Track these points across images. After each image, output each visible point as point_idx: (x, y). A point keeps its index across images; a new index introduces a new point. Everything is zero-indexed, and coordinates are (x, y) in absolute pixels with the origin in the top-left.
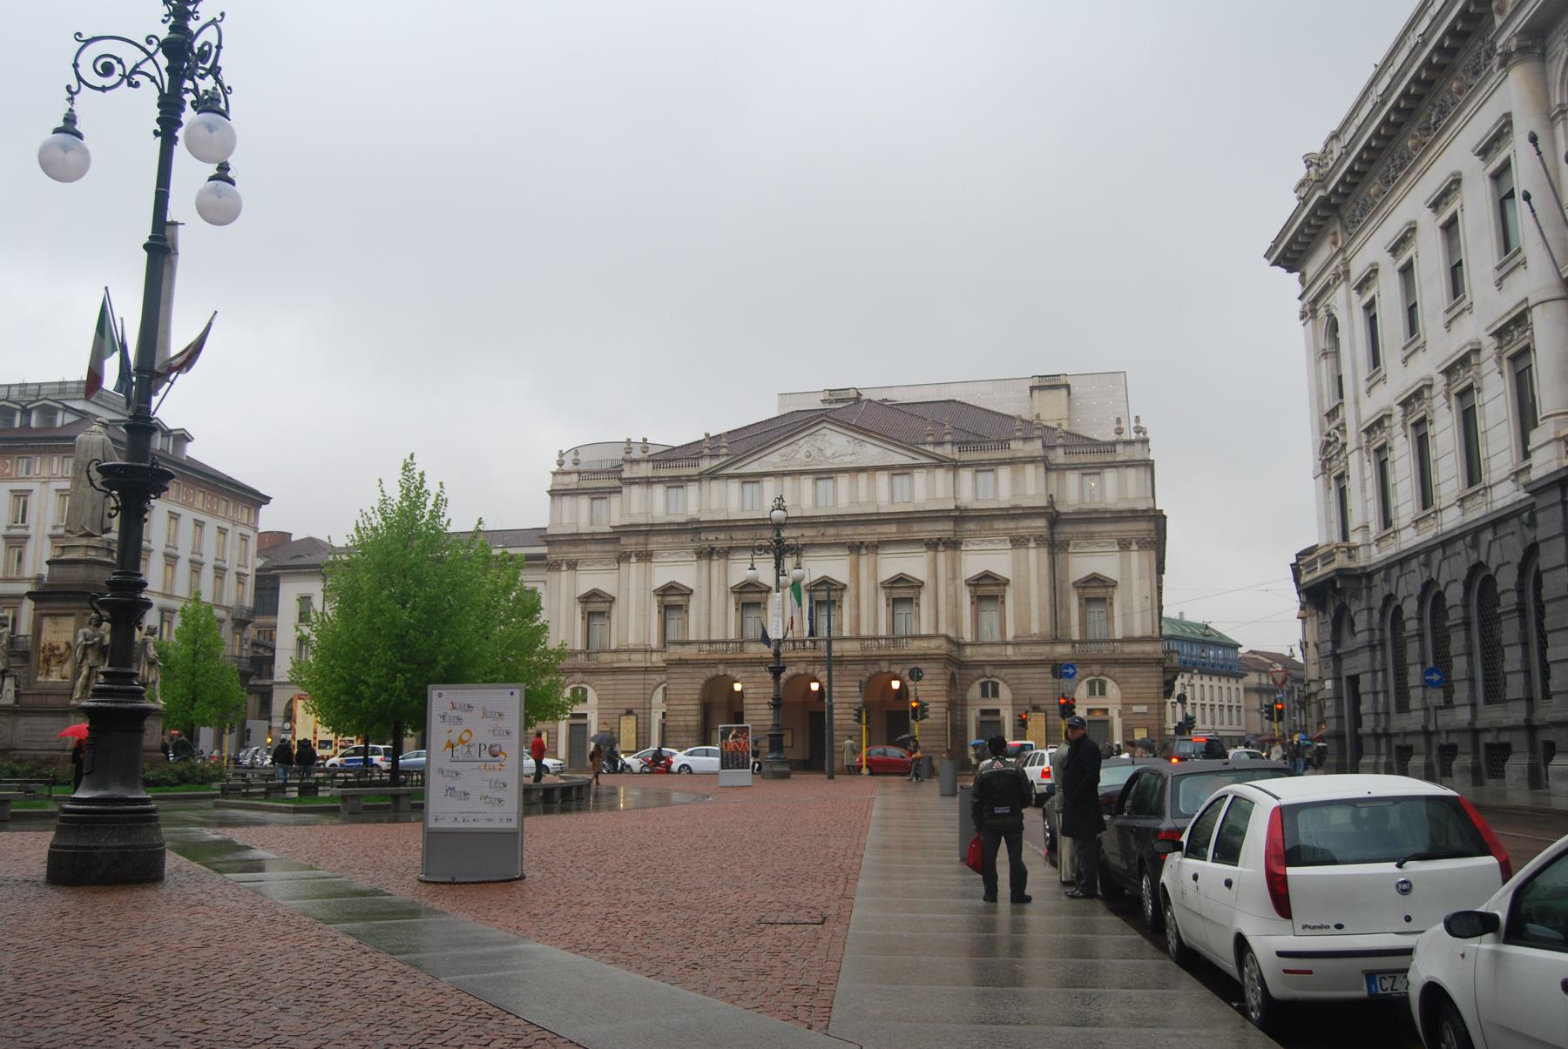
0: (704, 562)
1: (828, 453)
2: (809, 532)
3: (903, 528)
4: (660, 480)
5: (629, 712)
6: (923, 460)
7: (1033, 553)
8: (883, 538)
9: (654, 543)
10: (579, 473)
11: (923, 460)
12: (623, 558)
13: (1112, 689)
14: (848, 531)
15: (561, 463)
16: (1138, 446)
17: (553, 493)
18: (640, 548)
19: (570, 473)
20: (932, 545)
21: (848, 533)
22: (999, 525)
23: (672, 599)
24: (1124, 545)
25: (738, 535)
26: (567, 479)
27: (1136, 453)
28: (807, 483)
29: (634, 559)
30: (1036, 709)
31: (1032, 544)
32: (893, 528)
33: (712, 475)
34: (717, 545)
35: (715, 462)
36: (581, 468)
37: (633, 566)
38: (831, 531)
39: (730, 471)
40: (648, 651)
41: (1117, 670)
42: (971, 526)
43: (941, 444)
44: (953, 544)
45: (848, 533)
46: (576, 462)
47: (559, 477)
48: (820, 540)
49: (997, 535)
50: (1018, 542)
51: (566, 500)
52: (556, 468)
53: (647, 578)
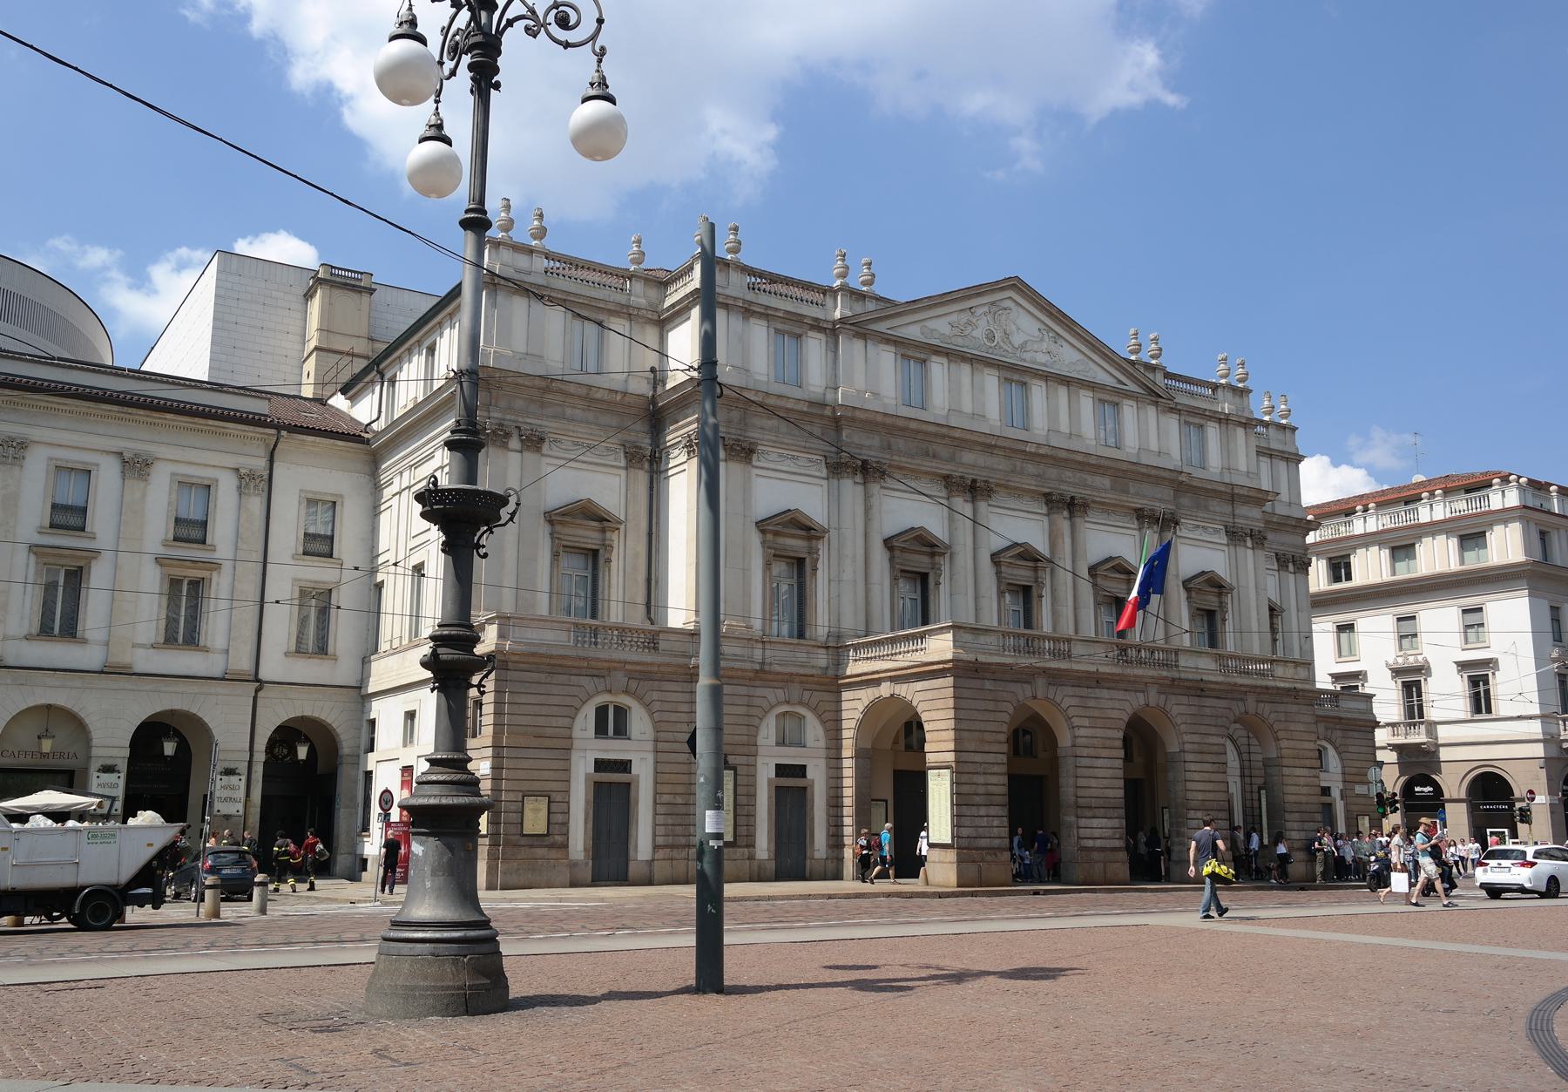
1: (1017, 339)
2: (1000, 463)
4: (767, 315)
6: (1132, 387)
7: (1250, 552)
9: (761, 429)
11: (1132, 387)
14: (1053, 472)
19: (530, 251)
20: (1143, 517)
22: (1216, 505)
23: (792, 544)
25: (901, 444)
26: (522, 261)
27: (1275, 441)
28: (991, 380)
32: (1107, 482)
35: (859, 308)
38: (1031, 468)
39: (882, 327)
42: (1185, 501)
44: (1168, 522)
49: (1213, 521)
50: (1235, 535)
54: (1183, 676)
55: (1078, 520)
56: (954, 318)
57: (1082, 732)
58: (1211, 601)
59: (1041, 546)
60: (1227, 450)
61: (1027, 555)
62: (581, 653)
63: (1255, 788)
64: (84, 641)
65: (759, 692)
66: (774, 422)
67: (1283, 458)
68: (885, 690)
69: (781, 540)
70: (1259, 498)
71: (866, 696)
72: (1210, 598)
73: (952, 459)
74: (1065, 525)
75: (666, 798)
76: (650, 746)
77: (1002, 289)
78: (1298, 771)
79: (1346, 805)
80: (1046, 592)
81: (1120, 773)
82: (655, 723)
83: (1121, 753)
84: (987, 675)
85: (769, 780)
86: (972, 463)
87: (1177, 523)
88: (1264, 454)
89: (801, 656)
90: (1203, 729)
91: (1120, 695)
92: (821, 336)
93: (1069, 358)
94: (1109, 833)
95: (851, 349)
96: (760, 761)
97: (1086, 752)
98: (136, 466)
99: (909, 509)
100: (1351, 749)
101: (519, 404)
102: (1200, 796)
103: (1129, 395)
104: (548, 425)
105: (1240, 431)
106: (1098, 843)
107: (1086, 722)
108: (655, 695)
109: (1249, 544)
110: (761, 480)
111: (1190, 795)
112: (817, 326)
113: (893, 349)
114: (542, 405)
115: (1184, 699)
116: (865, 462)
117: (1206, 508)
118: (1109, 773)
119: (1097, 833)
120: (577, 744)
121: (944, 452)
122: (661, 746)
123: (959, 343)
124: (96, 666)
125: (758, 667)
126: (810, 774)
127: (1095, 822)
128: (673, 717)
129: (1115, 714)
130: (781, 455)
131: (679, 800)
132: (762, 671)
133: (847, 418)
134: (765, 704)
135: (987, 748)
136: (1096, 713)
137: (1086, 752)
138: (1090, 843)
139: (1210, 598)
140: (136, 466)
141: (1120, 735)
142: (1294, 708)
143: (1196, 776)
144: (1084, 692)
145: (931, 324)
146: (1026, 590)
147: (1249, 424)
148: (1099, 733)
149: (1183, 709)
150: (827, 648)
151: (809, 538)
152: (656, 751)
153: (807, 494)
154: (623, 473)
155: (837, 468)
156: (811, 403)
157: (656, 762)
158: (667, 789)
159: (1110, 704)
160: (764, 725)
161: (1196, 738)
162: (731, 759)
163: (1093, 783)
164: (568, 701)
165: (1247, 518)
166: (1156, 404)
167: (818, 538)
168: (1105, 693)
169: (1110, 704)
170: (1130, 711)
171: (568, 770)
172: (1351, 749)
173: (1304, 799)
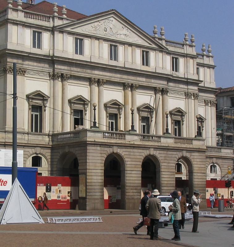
0: (57, 81)
3: (148, 80)
4: (29, 26)
8: (141, 84)
9: (28, 64)
11: (154, 46)
14: (125, 77)
21: (126, 79)
24: (206, 103)
32: (144, 79)
33: (62, 30)
34: (64, 72)
38: (119, 76)
39: (69, 29)
41: (220, 161)
43: (161, 39)
44: (164, 92)
45: (126, 79)
48: (113, 79)
50: (187, 95)
54: (162, 145)
55: (134, 92)
58: (178, 118)
59: (121, 100)
60: (186, 66)
61: (116, 104)
68: (67, 150)
70: (196, 83)
71: (61, 152)
72: (178, 116)
74: (129, 93)
80: (122, 116)
81: (140, 175)
83: (141, 169)
87: (168, 92)
89: (40, 138)
90: (167, 161)
95: (58, 36)
99: (76, 89)
102: (166, 182)
107: (130, 160)
109: (193, 98)
111: (163, 182)
112: (46, 29)
116: (62, 74)
121: (89, 71)
129: (138, 157)
134: (29, 155)
137: (129, 169)
139: (178, 116)
141: (141, 164)
143: (165, 176)
146: (116, 115)
149: (161, 155)
150: (49, 135)
153: (43, 86)
155: (53, 77)
156: (44, 56)
159: (137, 154)
163: (131, 178)
166: (161, 51)
168: (136, 150)
169: (137, 154)
170: (144, 156)
173: (200, 183)
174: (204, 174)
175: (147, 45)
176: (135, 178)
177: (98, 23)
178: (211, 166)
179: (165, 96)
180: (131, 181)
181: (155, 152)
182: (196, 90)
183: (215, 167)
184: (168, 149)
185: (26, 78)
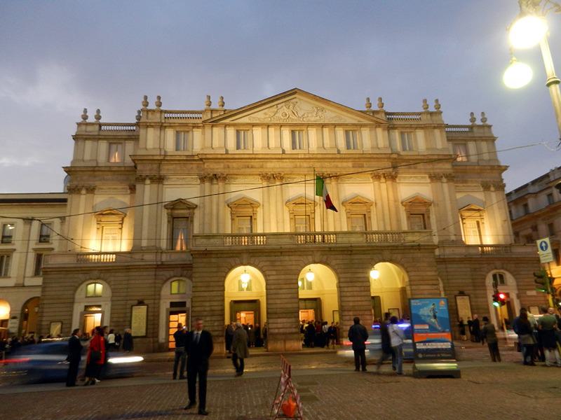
0: (207, 184)
2: (287, 165)
5: (141, 303)
6: (366, 122)
7: (445, 185)
10: (100, 125)
12: (142, 180)
13: (509, 278)
15: (85, 117)
16: (486, 129)
17: (76, 138)
18: (154, 173)
19: (92, 124)
22: (421, 166)
24: (486, 187)
26: (90, 128)
29: (148, 182)
30: (462, 293)
31: (444, 180)
32: (350, 164)
33: (214, 123)
36: (101, 121)
37: (147, 188)
39: (227, 121)
40: (158, 251)
46: (98, 117)
47: (83, 127)
49: (420, 173)
50: (435, 178)
51: (89, 144)
52: (80, 120)
53: (159, 194)
56: (266, 111)
57: (271, 278)
62: (78, 265)
63: (453, 296)
64: (10, 277)
65: (161, 273)
66: (174, 166)
67: (483, 140)
69: (176, 212)
73: (262, 167)
75: (115, 319)
76: (109, 299)
77: (290, 95)
78: (422, 287)
79: (521, 301)
82: (112, 289)
84: (213, 256)
85: (167, 309)
86: (272, 167)
88: (471, 140)
91: (297, 258)
92: (200, 130)
93: (329, 115)
94: (289, 325)
96: (162, 302)
97: (273, 287)
98: (29, 221)
100: (521, 273)
101: (85, 178)
102: (351, 304)
103: (365, 125)
104: (97, 183)
105: (437, 132)
106: (281, 331)
107: (274, 273)
108: (112, 278)
110: (167, 189)
113: (233, 128)
114: (95, 177)
115: (341, 257)
117: (415, 168)
118: (290, 295)
119: (279, 326)
120: (76, 300)
122: (115, 298)
123: (267, 121)
124: (12, 285)
125: (159, 263)
126: (187, 306)
127: (279, 320)
128: (120, 287)
130: (178, 178)
131: (121, 320)
132: (162, 265)
133: (205, 159)
135: (211, 289)
136: (281, 268)
137: (273, 287)
138: (276, 331)
140: (29, 221)
142: (419, 255)
143: (348, 294)
144: (273, 258)
145: (252, 115)
147: (441, 126)
148: (283, 277)
149: (338, 261)
151: (189, 208)
152: (112, 301)
154: (129, 196)
157: (112, 305)
158: (116, 315)
159: (290, 263)
160: (164, 286)
161: (349, 275)
162: (146, 302)
164: (73, 284)
165: (440, 169)
166: (379, 126)
167: (194, 208)
168: (287, 258)
169: (290, 263)
171: (72, 311)
172: (521, 273)
174: (435, 287)
175: (356, 122)
176: (286, 301)
177: (274, 109)
178: (494, 276)
179: (389, 183)
180: (279, 306)
181: (325, 257)
182: (448, 169)
183: (501, 277)
184: (351, 251)
185: (165, 186)
